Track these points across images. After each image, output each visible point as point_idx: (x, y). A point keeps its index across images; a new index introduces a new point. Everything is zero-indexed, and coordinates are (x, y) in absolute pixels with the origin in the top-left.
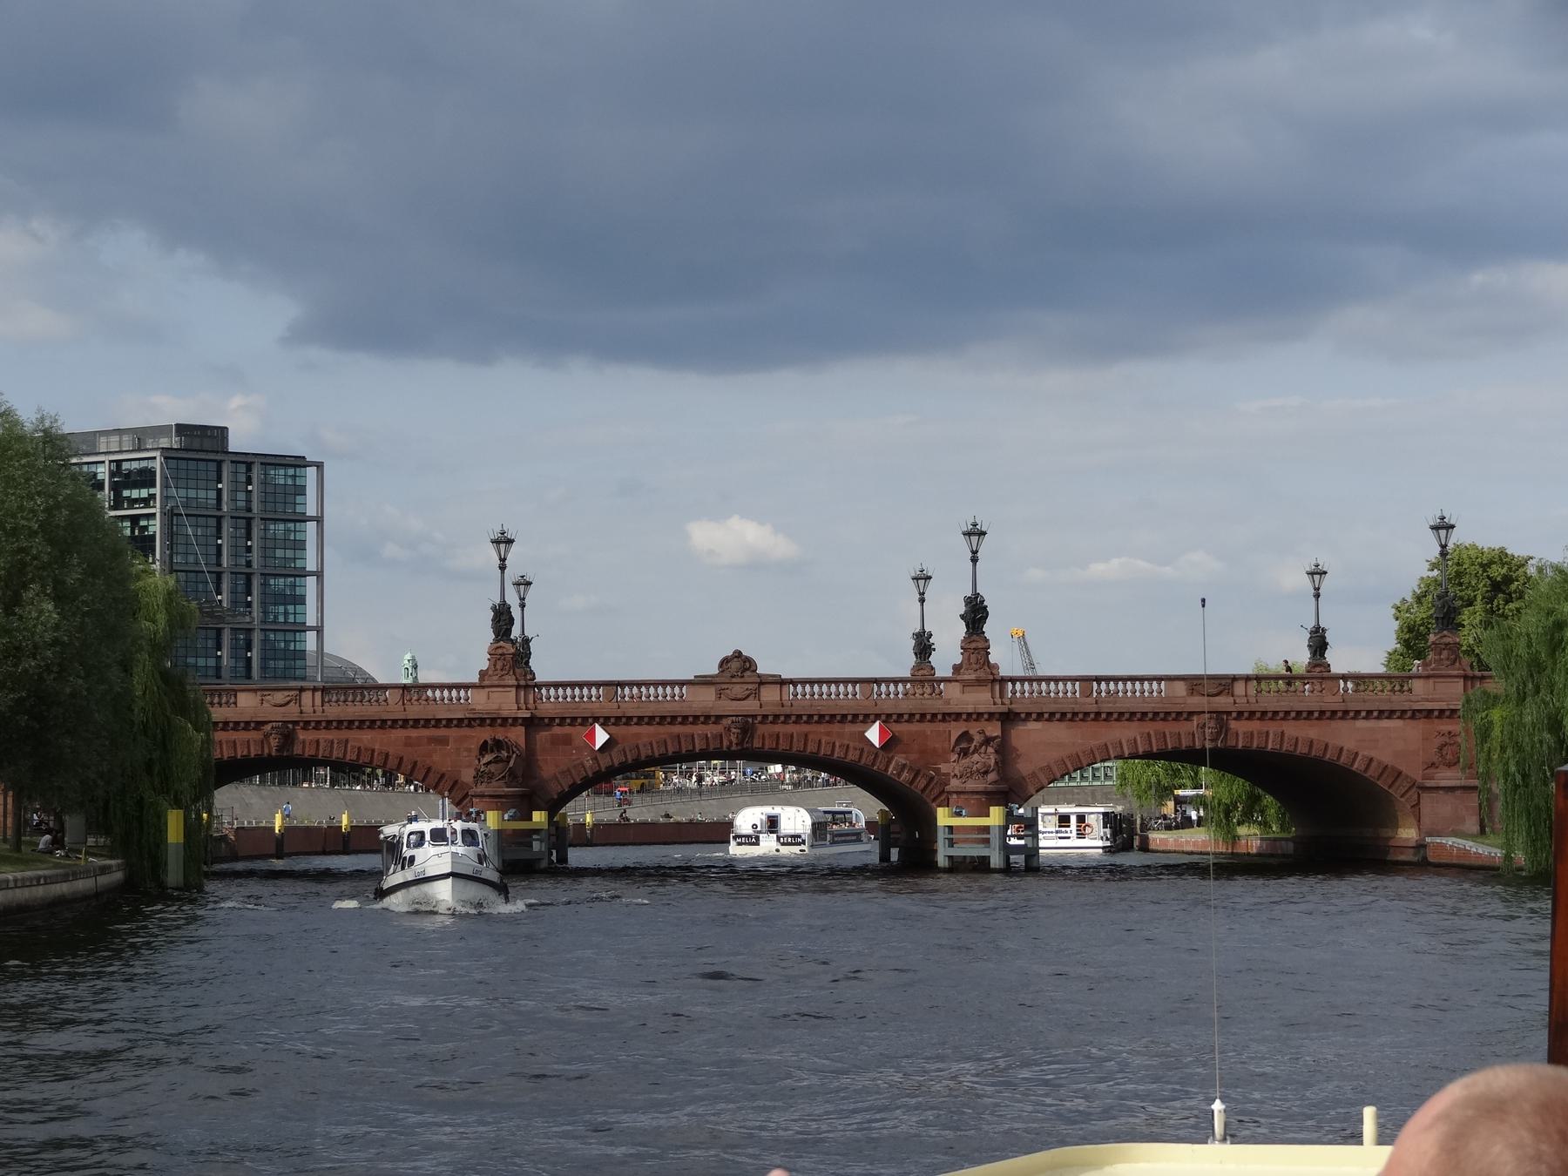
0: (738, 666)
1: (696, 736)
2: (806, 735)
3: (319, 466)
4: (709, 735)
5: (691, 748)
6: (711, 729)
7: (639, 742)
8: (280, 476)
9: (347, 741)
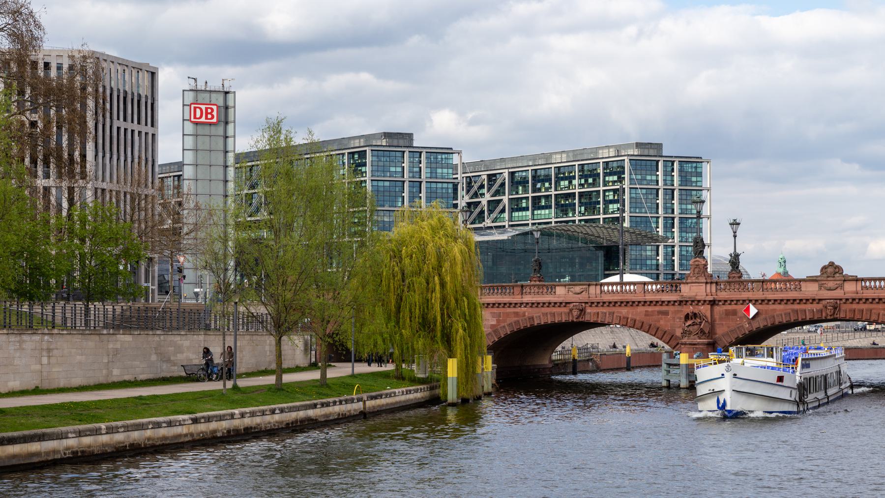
0: (832, 271)
1: (807, 311)
2: (871, 310)
4: (815, 310)
5: (804, 317)
6: (815, 307)
7: (775, 314)
9: (613, 313)
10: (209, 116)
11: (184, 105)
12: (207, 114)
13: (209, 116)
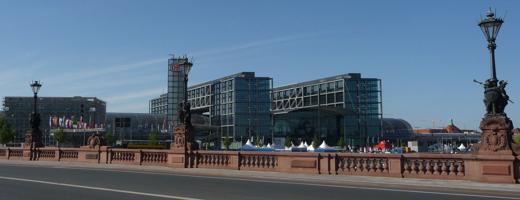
3: (380, 80)
8: (373, 83)
10: (178, 69)
11: (169, 65)
12: (177, 68)
13: (178, 69)
